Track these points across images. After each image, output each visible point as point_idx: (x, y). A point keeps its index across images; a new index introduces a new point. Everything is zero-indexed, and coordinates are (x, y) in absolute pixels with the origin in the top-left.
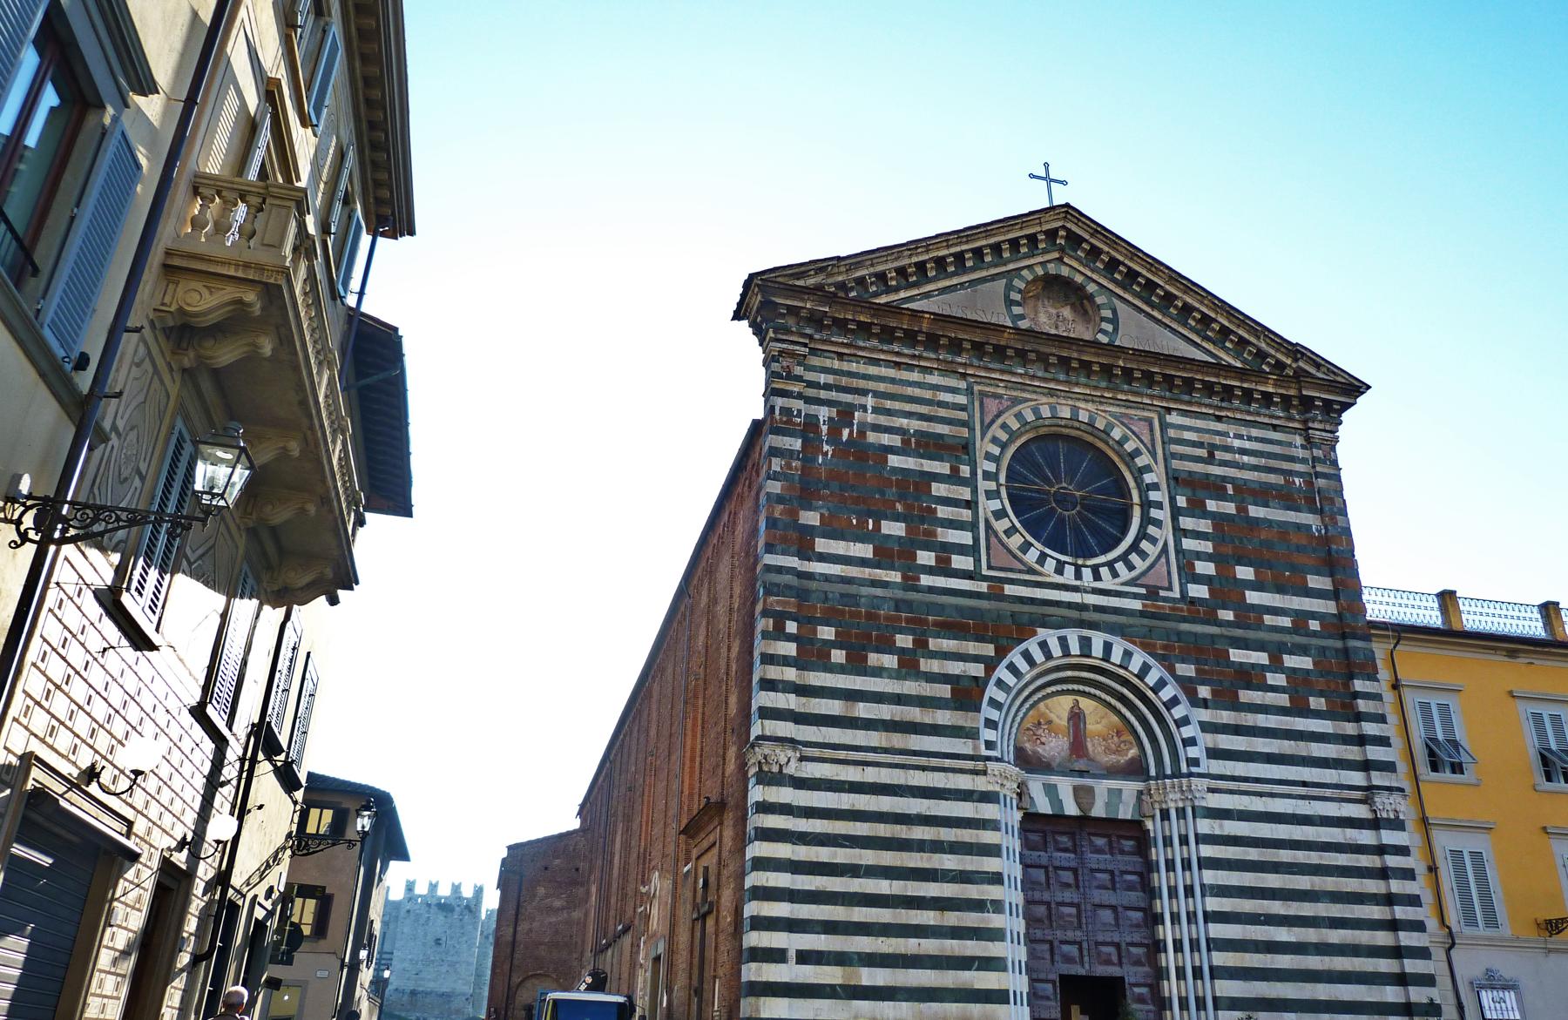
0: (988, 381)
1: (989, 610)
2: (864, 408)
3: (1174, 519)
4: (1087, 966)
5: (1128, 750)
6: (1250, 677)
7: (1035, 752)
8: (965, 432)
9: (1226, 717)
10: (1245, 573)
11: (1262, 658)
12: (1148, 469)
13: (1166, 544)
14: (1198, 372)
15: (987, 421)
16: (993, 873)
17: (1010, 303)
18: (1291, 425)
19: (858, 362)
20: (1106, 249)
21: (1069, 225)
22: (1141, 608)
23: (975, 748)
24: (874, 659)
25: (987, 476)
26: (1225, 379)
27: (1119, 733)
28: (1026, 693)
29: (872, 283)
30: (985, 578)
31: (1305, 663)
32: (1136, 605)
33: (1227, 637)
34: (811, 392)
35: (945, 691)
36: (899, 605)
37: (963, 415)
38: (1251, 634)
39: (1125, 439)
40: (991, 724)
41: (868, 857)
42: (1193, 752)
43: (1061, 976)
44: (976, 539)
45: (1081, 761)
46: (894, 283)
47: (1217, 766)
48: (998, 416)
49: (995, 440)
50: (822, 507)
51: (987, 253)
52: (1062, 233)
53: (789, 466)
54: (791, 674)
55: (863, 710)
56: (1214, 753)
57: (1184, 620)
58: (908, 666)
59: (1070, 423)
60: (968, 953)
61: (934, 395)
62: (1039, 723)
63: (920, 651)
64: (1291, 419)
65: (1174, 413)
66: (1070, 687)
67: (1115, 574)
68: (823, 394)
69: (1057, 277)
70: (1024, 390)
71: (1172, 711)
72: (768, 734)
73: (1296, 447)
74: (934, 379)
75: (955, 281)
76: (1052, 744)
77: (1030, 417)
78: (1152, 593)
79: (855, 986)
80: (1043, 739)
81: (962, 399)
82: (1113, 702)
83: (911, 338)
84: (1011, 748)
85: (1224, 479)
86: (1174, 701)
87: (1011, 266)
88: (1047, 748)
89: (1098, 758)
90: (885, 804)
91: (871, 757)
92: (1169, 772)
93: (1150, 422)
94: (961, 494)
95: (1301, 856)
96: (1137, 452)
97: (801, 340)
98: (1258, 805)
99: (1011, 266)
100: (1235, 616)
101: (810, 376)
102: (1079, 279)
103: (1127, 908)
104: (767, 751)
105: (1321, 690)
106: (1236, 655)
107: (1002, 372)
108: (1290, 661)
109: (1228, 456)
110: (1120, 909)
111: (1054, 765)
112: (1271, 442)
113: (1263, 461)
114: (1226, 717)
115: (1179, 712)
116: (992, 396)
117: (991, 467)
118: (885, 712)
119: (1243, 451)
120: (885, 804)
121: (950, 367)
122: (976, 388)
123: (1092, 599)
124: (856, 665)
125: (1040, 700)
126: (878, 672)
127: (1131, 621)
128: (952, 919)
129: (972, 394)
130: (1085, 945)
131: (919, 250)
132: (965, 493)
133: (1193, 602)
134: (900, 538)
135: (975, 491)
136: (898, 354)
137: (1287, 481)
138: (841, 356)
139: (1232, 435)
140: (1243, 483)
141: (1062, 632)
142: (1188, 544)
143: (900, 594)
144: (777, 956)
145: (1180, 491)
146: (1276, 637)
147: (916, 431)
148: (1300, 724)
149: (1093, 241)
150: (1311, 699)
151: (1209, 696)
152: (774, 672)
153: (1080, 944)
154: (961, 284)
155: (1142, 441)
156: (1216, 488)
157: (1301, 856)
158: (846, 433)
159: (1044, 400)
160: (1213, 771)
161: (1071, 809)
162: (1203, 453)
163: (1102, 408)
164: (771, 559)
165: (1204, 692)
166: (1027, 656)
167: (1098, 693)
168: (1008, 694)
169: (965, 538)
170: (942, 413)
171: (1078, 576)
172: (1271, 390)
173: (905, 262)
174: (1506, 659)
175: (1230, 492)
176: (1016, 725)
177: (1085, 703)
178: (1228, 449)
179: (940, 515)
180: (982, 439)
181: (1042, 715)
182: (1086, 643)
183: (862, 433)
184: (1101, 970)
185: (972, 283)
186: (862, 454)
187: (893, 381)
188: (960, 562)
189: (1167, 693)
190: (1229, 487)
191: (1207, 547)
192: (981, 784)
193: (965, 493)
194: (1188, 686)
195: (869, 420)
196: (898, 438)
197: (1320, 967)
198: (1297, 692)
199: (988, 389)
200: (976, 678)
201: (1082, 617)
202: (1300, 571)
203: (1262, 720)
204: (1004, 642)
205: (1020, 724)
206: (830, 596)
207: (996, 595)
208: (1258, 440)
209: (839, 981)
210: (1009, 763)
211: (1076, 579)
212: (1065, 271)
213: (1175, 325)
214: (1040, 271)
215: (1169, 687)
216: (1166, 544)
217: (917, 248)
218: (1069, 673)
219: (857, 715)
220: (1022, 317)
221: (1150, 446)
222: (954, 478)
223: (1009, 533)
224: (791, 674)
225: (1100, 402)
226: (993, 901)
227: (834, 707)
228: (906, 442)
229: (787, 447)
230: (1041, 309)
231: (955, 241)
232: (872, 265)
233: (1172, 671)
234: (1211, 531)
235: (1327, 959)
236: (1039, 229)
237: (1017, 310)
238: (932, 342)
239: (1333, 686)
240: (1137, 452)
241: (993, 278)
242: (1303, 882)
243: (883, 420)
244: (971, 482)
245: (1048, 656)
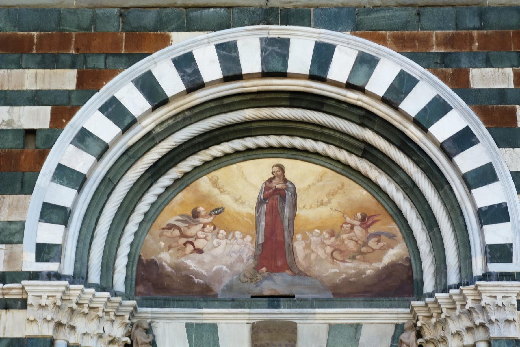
5: (384, 250)
7: (177, 268)
23: (10, 258)
45: (278, 277)
66: (262, 141)
71: (457, 159)
76: (218, 251)
80: (199, 244)
82: (353, 160)
88: (206, 257)
89: (317, 270)
92: (453, 279)
111: (218, 289)
167: (320, 147)
168: (100, 157)
181: (204, 198)
200: (31, 133)
204: (100, 63)
218: (250, 114)
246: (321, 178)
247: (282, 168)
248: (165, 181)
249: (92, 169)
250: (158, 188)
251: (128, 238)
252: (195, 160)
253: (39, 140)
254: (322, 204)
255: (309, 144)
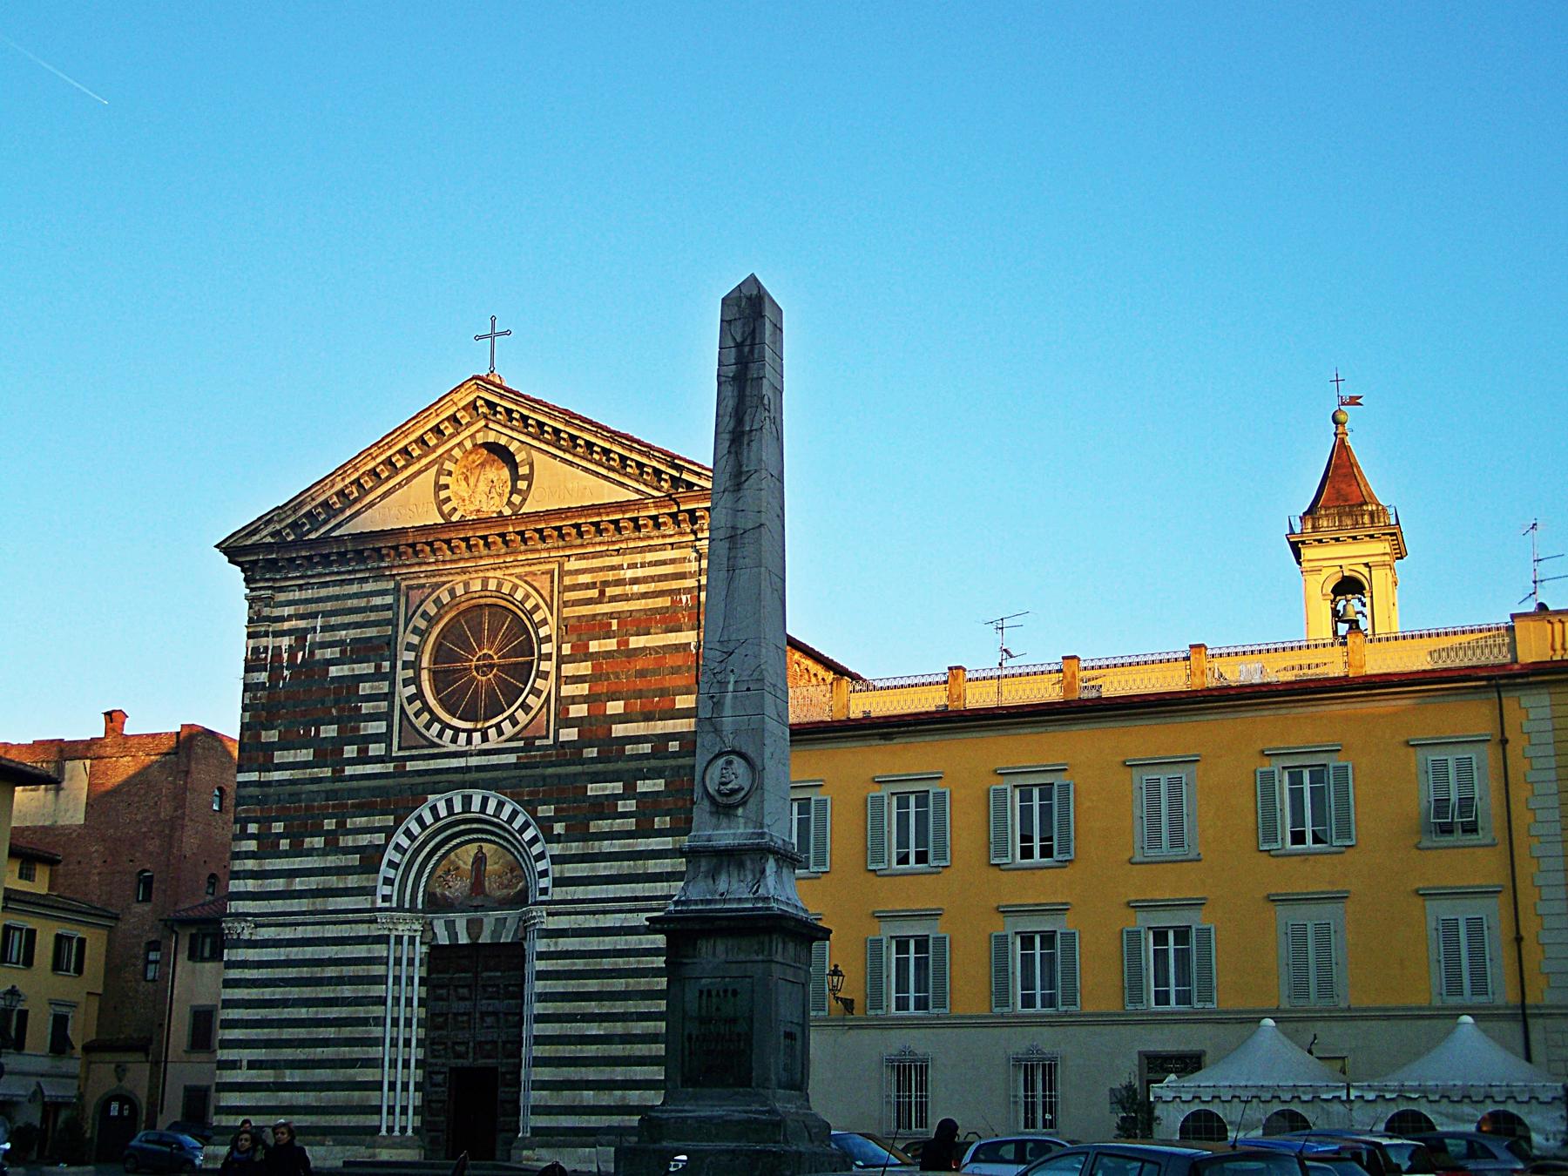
0: (412, 576)
1: (391, 787)
2: (314, 629)
3: (558, 668)
4: (471, 1060)
5: (518, 883)
6: (605, 807)
7: (443, 895)
8: (389, 630)
9: (575, 848)
10: (615, 707)
11: (617, 787)
12: (544, 622)
13: (549, 694)
14: (580, 516)
15: (410, 614)
16: (377, 997)
17: (440, 487)
18: (685, 539)
19: (313, 588)
20: (514, 407)
21: (481, 395)
22: (515, 761)
24: (309, 842)
25: (406, 665)
26: (608, 514)
27: (512, 871)
28: (427, 849)
29: (319, 513)
30: (393, 759)
31: (658, 785)
32: (512, 758)
33: (588, 773)
34: (278, 626)
35: (355, 859)
36: (329, 795)
37: (389, 614)
38: (611, 767)
39: (527, 596)
40: (388, 881)
41: (295, 992)
42: (544, 882)
43: (451, 1069)
44: (390, 727)
46: (338, 506)
47: (559, 893)
48: (419, 607)
49: (415, 631)
50: (280, 725)
51: (413, 449)
52: (480, 403)
53: (255, 697)
54: (250, 864)
55: (299, 884)
56: (559, 882)
57: (552, 764)
58: (332, 847)
59: (483, 594)
60: (354, 1056)
61: (368, 602)
62: (449, 870)
63: (340, 831)
64: (682, 534)
65: (572, 559)
67: (500, 732)
68: (287, 625)
69: (486, 445)
70: (441, 575)
72: (233, 911)
73: (690, 561)
74: (368, 587)
75: (392, 483)
77: (446, 598)
78: (529, 744)
79: (281, 1083)
80: (451, 884)
81: (389, 600)
82: (505, 844)
83: (342, 558)
84: (420, 894)
85: (611, 615)
86: (535, 840)
87: (440, 451)
88: (453, 890)
90: (309, 952)
91: (300, 919)
93: (552, 573)
94: (381, 689)
95: (621, 962)
96: (537, 607)
97: (266, 585)
98: (590, 922)
99: (440, 451)
100: (598, 752)
101: (277, 612)
102: (503, 441)
103: (506, 1014)
104: (230, 925)
105: (669, 810)
106: (593, 789)
107: (420, 564)
108: (643, 786)
109: (617, 591)
110: (501, 1015)
111: (456, 903)
112: (664, 563)
113: (652, 587)
114: (575, 848)
115: (536, 849)
116: (416, 588)
117: (410, 656)
118: (313, 883)
119: (635, 581)
120: (309, 952)
121: (379, 572)
122: (403, 584)
123: (474, 761)
124: (297, 851)
125: (449, 852)
126: (310, 852)
127: (505, 774)
128: (346, 1032)
129: (399, 590)
130: (471, 1044)
131: (349, 472)
132: (384, 687)
133: (560, 745)
134: (334, 737)
135: (393, 684)
136: (338, 573)
137: (672, 601)
138: (300, 587)
139: (625, 567)
140: (628, 614)
141: (448, 795)
142: (567, 690)
143: (328, 786)
144: (233, 1065)
145: (566, 638)
146: (633, 765)
147: (351, 640)
148: (642, 844)
149: (504, 403)
150: (656, 819)
151: (563, 832)
152: (238, 865)
153: (468, 1043)
154: (399, 483)
155: (541, 596)
156: (599, 627)
157: (621, 962)
158: (300, 655)
159: (459, 578)
160: (555, 898)
161: (463, 939)
162: (594, 593)
163: (508, 572)
164: (242, 777)
165: (559, 828)
166: (420, 820)
168: (404, 855)
169: (381, 727)
170: (373, 616)
171: (469, 741)
172: (654, 512)
173: (339, 486)
174: (883, 742)
175: (614, 627)
176: (426, 875)
177: (486, 847)
178: (619, 582)
179: (363, 712)
180: (405, 632)
181: (452, 862)
182: (467, 801)
183: (312, 653)
184: (481, 1062)
185: (409, 479)
186: (312, 670)
187: (337, 598)
188: (376, 749)
189: (528, 835)
190: (615, 622)
191: (583, 689)
192: (375, 930)
193: (384, 687)
194: (545, 825)
195: (317, 640)
196: (338, 649)
197: (621, 1054)
198: (645, 814)
199: (412, 582)
201: (464, 779)
202: (667, 693)
203: (607, 846)
204: (401, 812)
205: (431, 873)
206: (282, 797)
207: (400, 772)
208: (652, 564)
209: (272, 1080)
210: (413, 909)
211: (467, 744)
212: (492, 437)
213: (584, 463)
214: (468, 445)
215: (531, 828)
216: (549, 694)
217: (345, 472)
219: (293, 888)
220: (448, 499)
221: (548, 599)
222: (378, 676)
223: (417, 715)
224: (250, 864)
225: (507, 567)
226: (374, 1018)
227: (279, 884)
228: (343, 652)
229: (256, 681)
230: (482, 478)
231: (378, 452)
232: (313, 499)
233: (533, 814)
234: (589, 672)
235: (628, 1046)
236: (455, 409)
237: (443, 494)
238: (360, 556)
239: (680, 803)
240: (537, 607)
241: (427, 467)
242: (619, 984)
243: (328, 637)
244: (390, 677)
245: (437, 818)
246: (496, 850)
247: (481, 847)
248: (436, 858)
249: (401, 860)
250: (433, 861)
251: (422, 885)
252: (447, 848)
253: (381, 849)
254: (496, 863)
255: (489, 837)
